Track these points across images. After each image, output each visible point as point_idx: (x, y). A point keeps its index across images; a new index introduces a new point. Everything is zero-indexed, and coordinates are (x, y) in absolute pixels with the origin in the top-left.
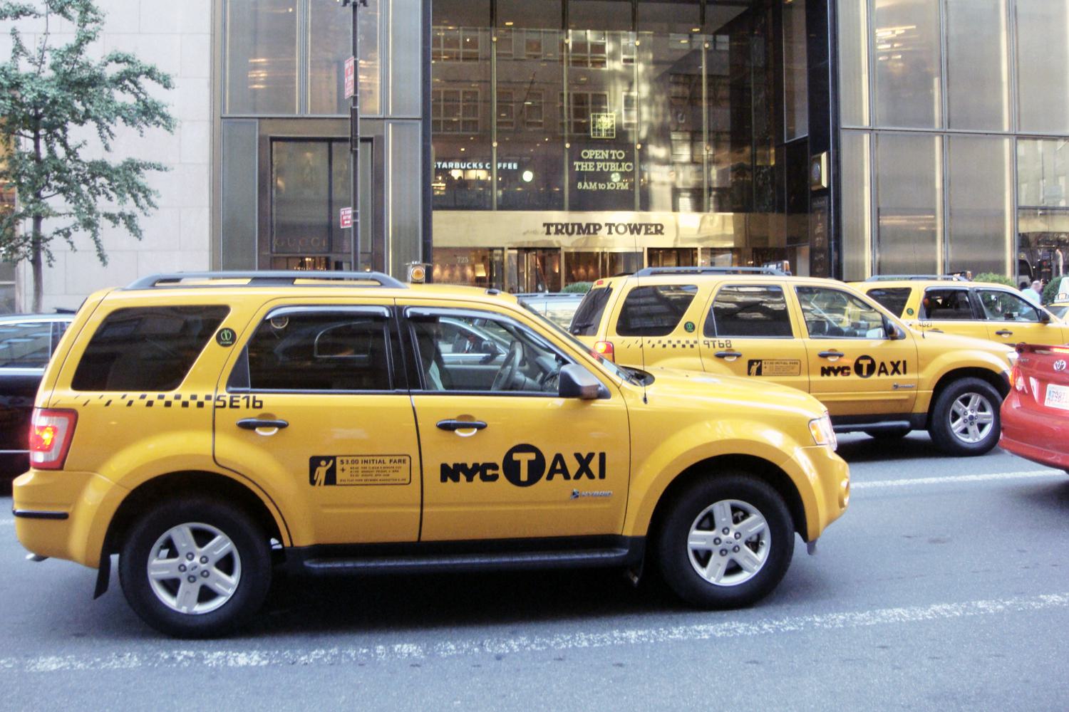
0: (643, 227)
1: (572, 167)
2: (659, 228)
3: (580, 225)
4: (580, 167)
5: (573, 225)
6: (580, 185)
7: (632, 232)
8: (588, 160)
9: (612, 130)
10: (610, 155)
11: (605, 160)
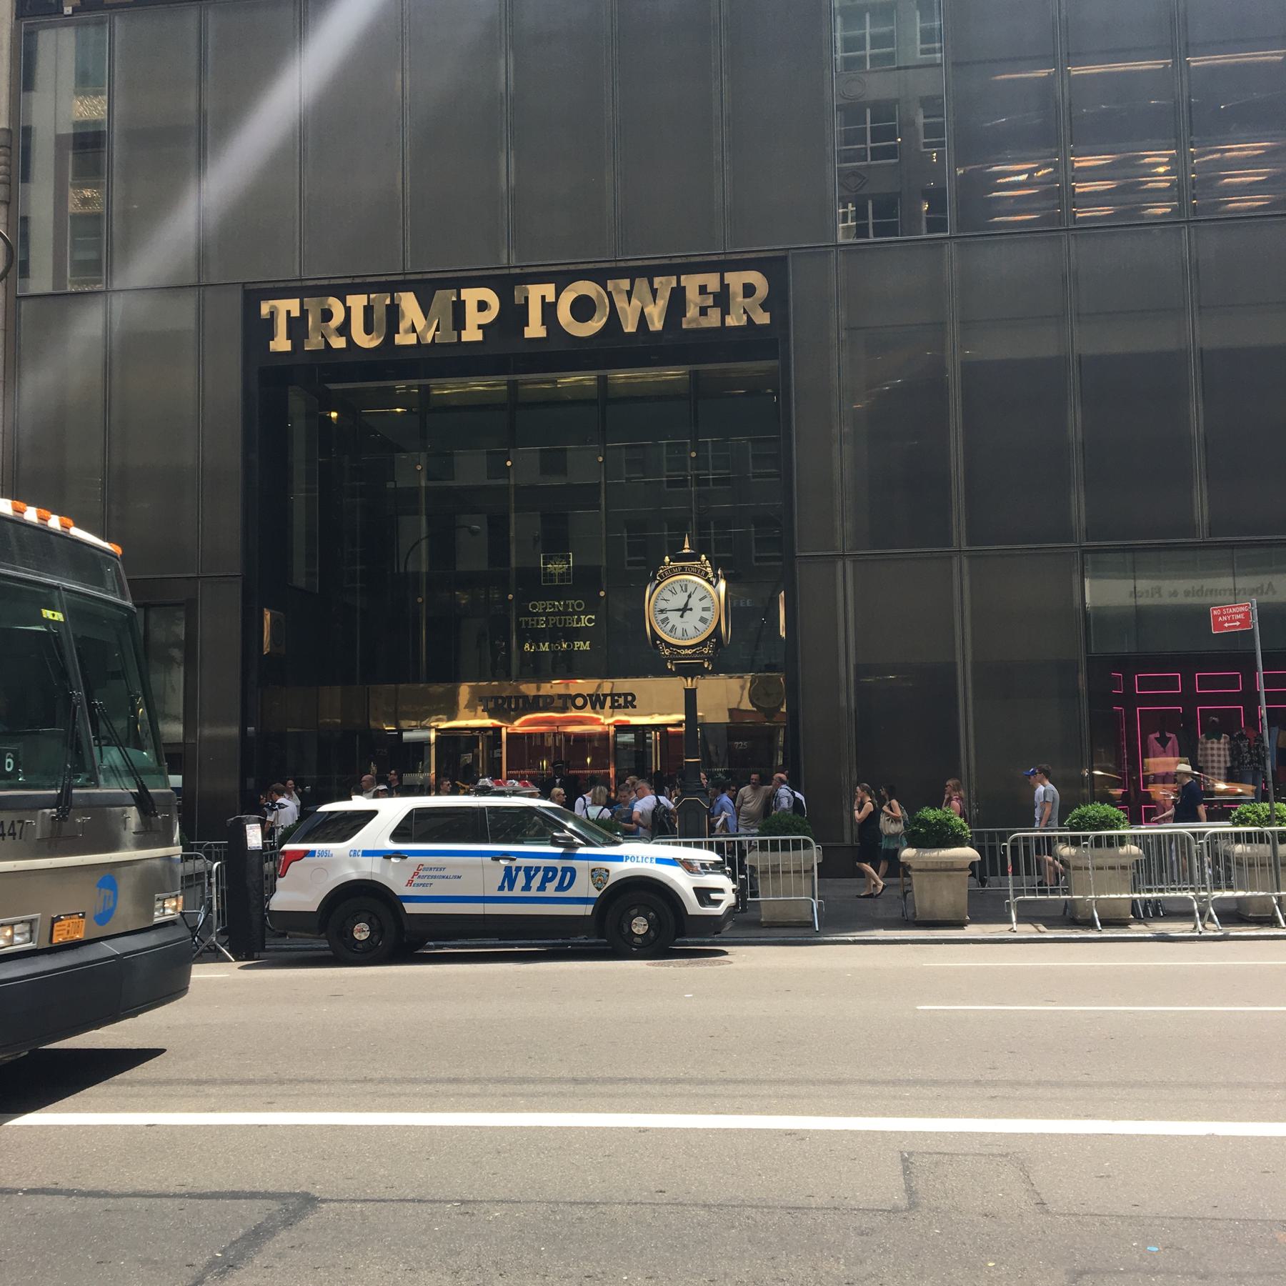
0: (609, 699)
1: (519, 624)
2: (630, 698)
3: (526, 697)
4: (527, 623)
5: (517, 698)
6: (527, 646)
7: (593, 707)
8: (538, 614)
9: (568, 574)
10: (566, 606)
11: (559, 613)
